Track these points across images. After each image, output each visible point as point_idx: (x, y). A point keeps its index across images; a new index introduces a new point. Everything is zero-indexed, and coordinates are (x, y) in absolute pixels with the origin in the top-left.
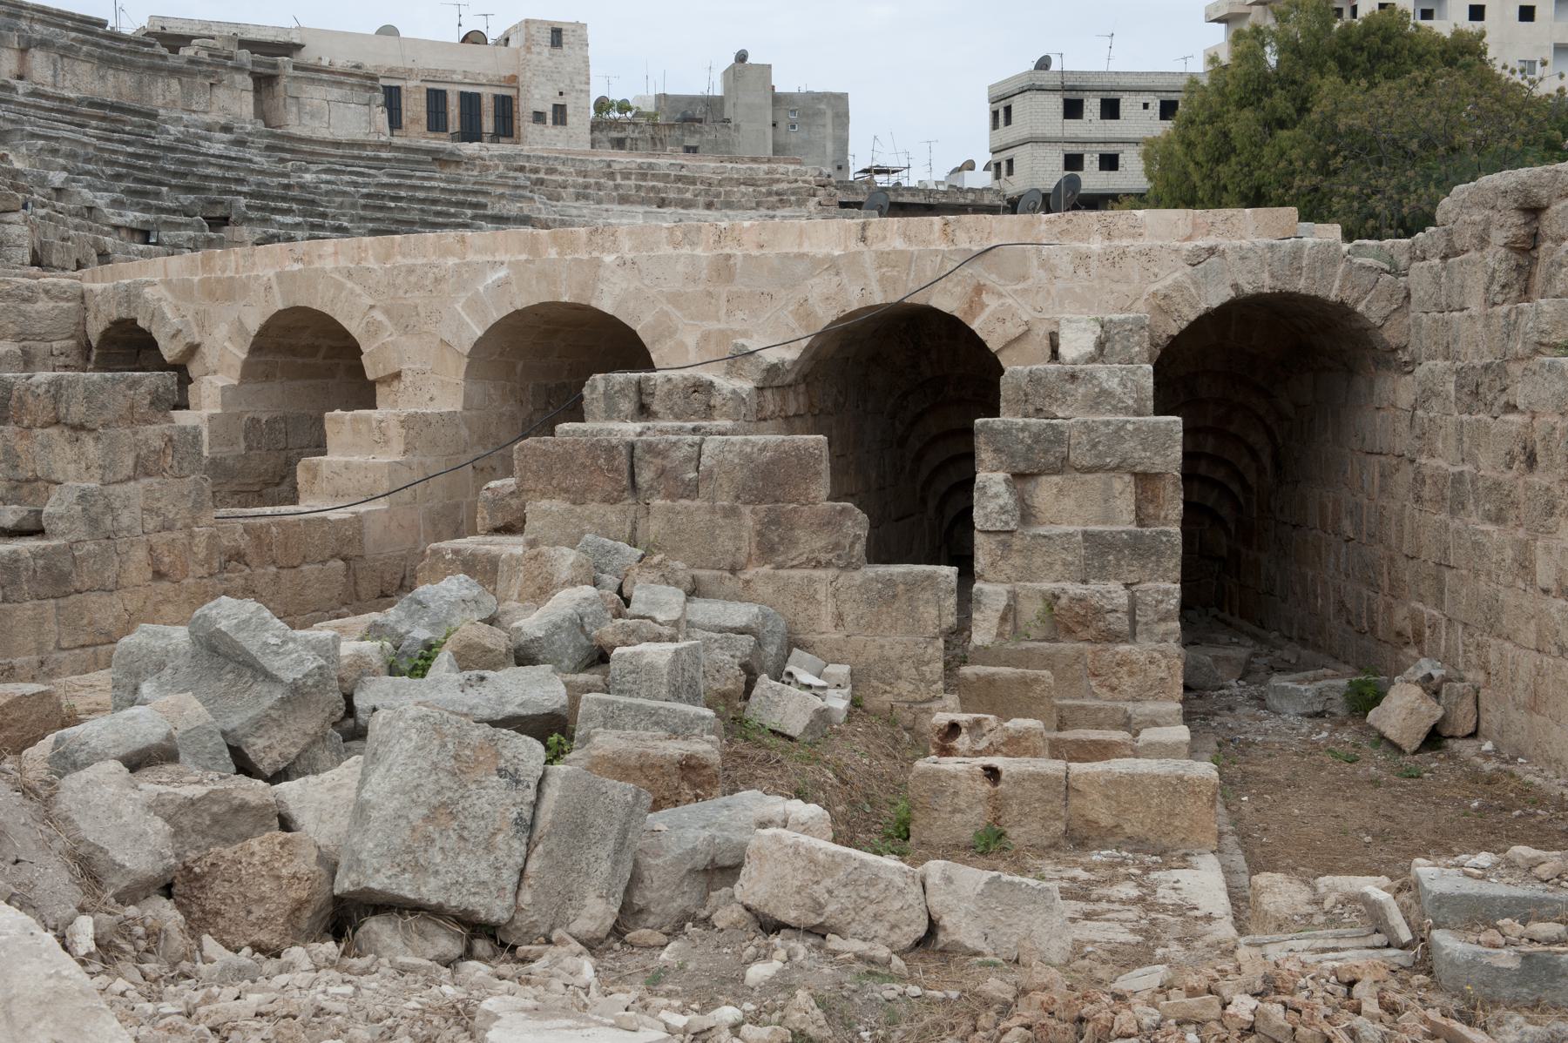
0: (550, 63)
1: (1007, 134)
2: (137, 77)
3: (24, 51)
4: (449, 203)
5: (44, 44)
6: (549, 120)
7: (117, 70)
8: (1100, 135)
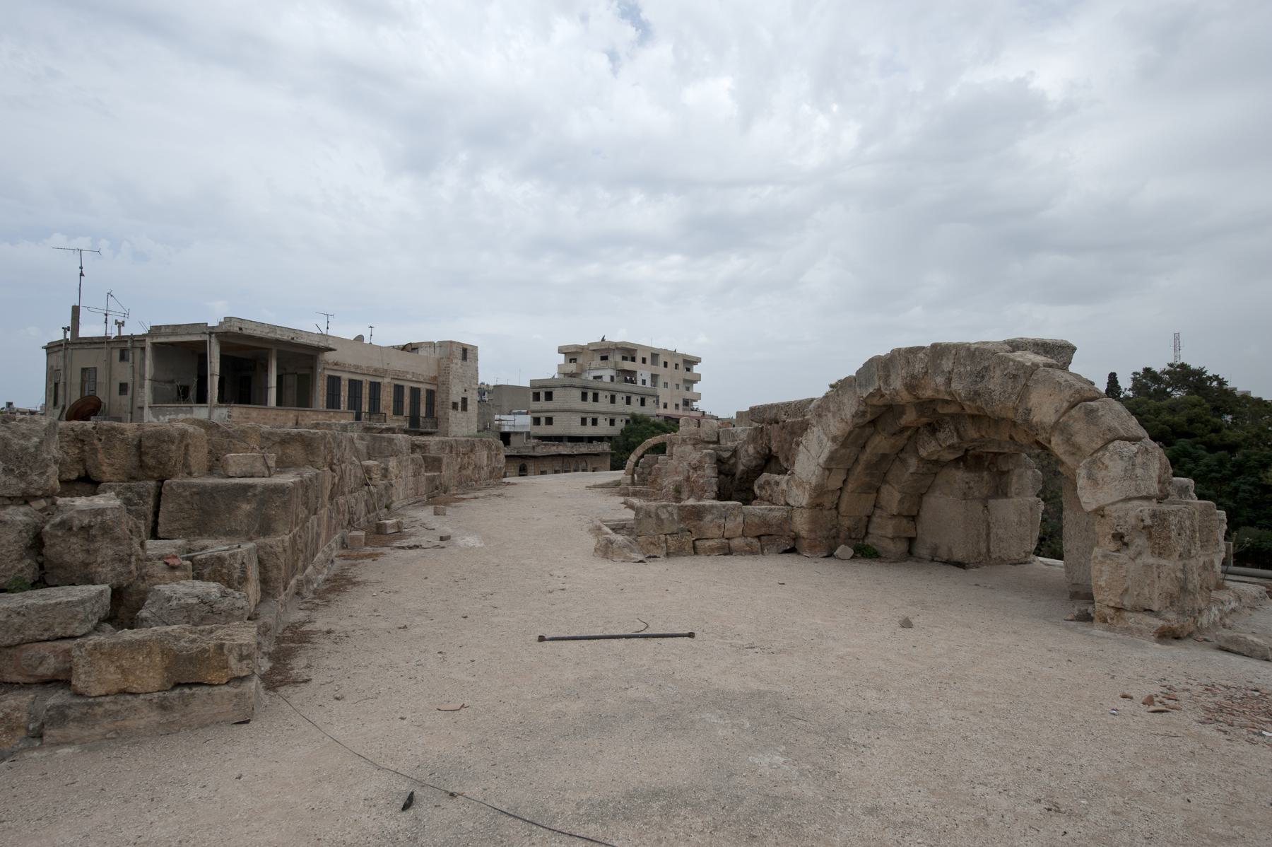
0: (461, 371)
1: (543, 404)
6: (460, 409)
8: (592, 409)
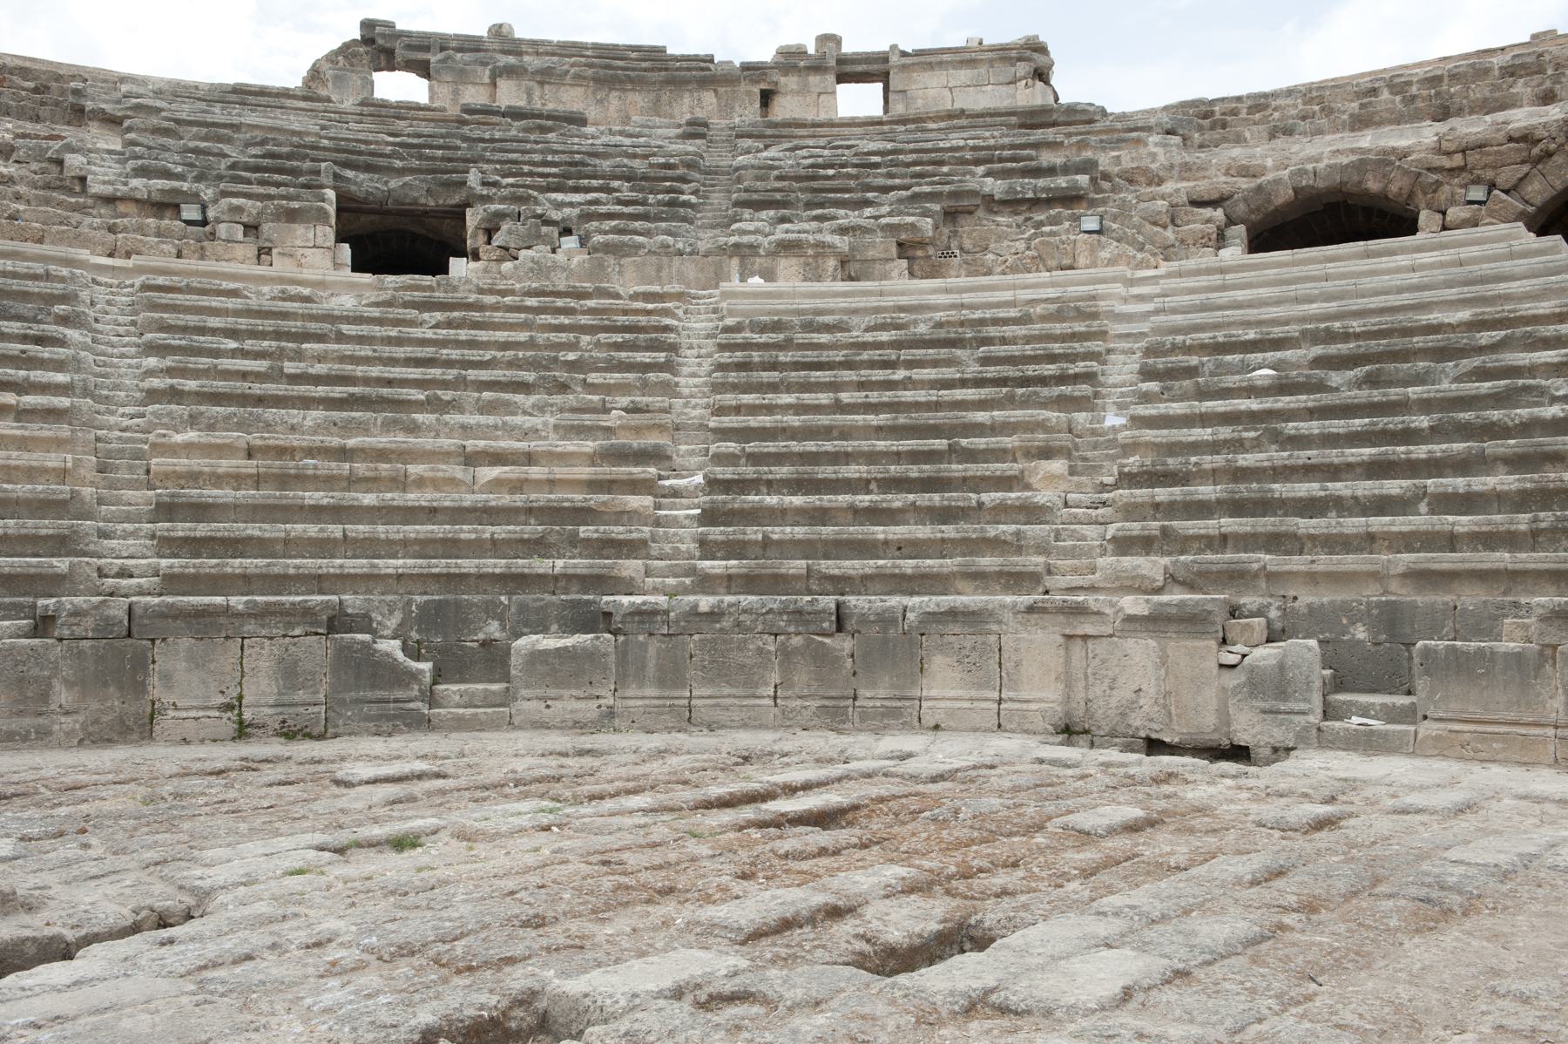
2: (652, 96)
3: (494, 85)
4: (964, 162)
5: (511, 72)
7: (624, 90)
